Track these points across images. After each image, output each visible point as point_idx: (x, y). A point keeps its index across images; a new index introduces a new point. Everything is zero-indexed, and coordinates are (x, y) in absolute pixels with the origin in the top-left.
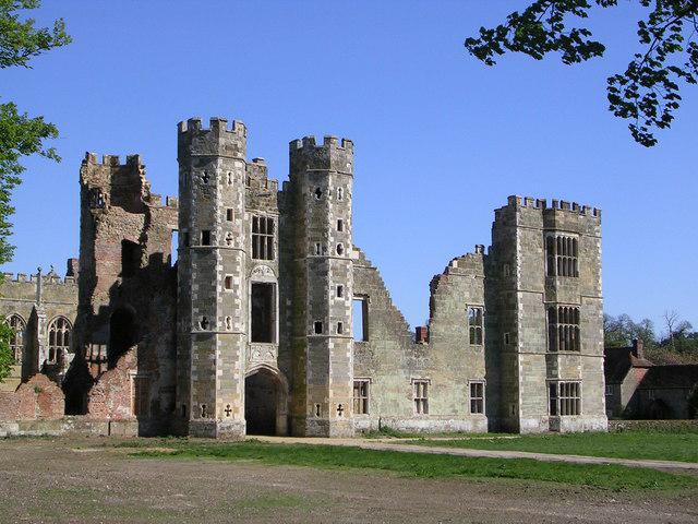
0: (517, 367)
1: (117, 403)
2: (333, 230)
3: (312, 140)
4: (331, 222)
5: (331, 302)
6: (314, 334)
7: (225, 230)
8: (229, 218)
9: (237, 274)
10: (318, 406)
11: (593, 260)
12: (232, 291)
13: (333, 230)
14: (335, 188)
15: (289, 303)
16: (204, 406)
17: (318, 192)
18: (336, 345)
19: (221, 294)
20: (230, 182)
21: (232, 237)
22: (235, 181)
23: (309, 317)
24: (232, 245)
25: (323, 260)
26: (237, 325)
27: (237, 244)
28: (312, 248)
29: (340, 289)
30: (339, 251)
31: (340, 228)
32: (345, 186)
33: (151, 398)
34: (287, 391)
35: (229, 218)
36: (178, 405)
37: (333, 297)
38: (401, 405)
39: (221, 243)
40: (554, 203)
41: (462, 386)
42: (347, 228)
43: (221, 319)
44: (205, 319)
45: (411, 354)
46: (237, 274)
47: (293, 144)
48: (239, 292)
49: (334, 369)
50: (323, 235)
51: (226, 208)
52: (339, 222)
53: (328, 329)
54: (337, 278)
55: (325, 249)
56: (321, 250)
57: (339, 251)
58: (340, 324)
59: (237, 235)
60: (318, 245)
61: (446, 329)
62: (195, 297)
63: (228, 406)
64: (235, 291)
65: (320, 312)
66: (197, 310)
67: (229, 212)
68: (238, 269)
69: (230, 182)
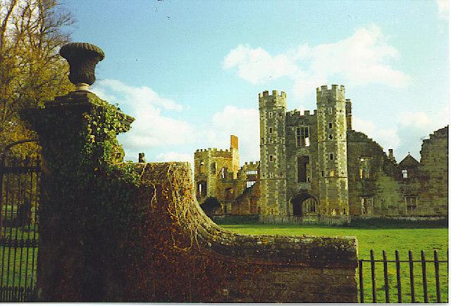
2: (326, 129)
7: (268, 137)
18: (330, 181)
19: (267, 163)
24: (272, 142)
30: (331, 137)
31: (331, 127)
37: (327, 159)
42: (335, 126)
48: (276, 162)
52: (330, 125)
57: (331, 137)
68: (276, 152)
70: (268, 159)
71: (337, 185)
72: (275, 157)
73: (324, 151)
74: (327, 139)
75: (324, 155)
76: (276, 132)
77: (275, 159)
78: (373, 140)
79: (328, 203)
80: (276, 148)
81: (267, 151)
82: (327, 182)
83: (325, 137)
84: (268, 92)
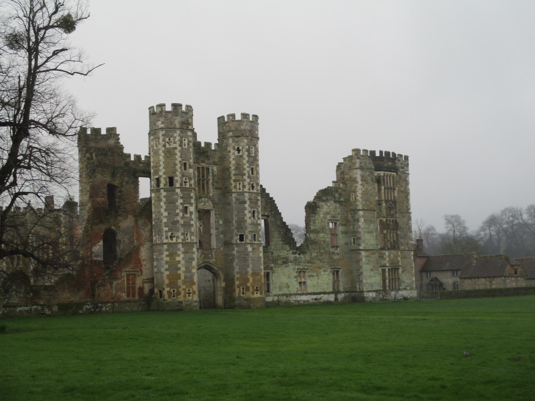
0: (361, 259)
1: (117, 290)
3: (233, 116)
5: (249, 221)
6: (238, 242)
8: (185, 169)
10: (243, 288)
11: (405, 189)
13: (249, 174)
15: (221, 222)
16: (174, 291)
17: (238, 150)
18: (253, 249)
19: (182, 218)
21: (187, 180)
22: (188, 144)
23: (235, 231)
25: (242, 194)
26: (193, 238)
28: (235, 187)
29: (254, 212)
33: (137, 286)
34: (222, 279)
35: (185, 169)
36: (156, 291)
37: (250, 218)
38: (291, 287)
39: (181, 184)
40: (381, 152)
41: (327, 273)
43: (183, 234)
44: (172, 234)
45: (295, 253)
46: (191, 204)
47: (221, 119)
48: (193, 217)
49: (252, 264)
50: (243, 178)
51: (184, 162)
52: (252, 169)
53: (247, 238)
55: (244, 187)
56: (241, 187)
57: (253, 187)
58: (255, 235)
59: (190, 179)
60: (240, 184)
61: (317, 236)
62: (165, 220)
63: (189, 290)
64: (191, 216)
65: (242, 228)
66: (167, 229)
67: (185, 164)
70: (181, 211)
73: (246, 206)
74: (249, 189)
75: (246, 212)
77: (191, 213)
78: (271, 196)
79: (251, 279)
80: (192, 194)
81: (181, 198)
82: (250, 249)
83: (247, 187)
84: (180, 105)
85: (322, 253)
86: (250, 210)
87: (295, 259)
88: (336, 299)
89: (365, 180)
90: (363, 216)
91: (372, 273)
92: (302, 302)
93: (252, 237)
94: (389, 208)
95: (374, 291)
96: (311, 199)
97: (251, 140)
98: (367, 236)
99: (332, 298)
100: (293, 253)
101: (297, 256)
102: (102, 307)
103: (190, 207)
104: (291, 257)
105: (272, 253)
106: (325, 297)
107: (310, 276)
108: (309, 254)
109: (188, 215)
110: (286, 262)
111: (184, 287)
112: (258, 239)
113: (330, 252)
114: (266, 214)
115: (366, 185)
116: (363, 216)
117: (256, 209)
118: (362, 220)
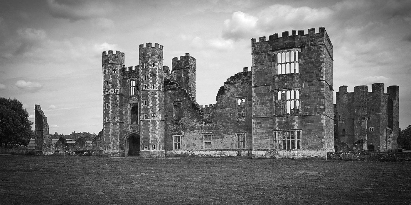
4: (142, 77)
9: (109, 102)
12: (108, 108)
14: (143, 64)
20: (107, 72)
22: (109, 71)
27: (109, 93)
32: (147, 62)
37: (142, 106)
38: (197, 145)
41: (231, 136)
42: (148, 78)
45: (202, 123)
46: (109, 102)
48: (110, 109)
54: (144, 98)
59: (109, 89)
64: (109, 109)
68: (110, 101)
69: (107, 72)
71: (149, 126)
72: (110, 105)
76: (110, 85)
85: (227, 122)
86: (142, 101)
87: (202, 127)
88: (239, 155)
89: (260, 62)
90: (255, 92)
91: (264, 136)
92: (206, 156)
93: (143, 117)
94: (282, 80)
95: (263, 150)
96: (223, 85)
97: (144, 59)
98: (259, 107)
99: (235, 154)
100: (200, 124)
101: (203, 125)
102: (92, 153)
103: (109, 104)
104: (198, 126)
105: (183, 124)
106: (228, 153)
107: (214, 138)
108: (214, 123)
109: (108, 108)
110: (193, 129)
111: (105, 145)
112: (148, 117)
113: (235, 121)
114: (179, 100)
115: (260, 67)
116: (255, 92)
117: (147, 100)
118: (254, 95)
